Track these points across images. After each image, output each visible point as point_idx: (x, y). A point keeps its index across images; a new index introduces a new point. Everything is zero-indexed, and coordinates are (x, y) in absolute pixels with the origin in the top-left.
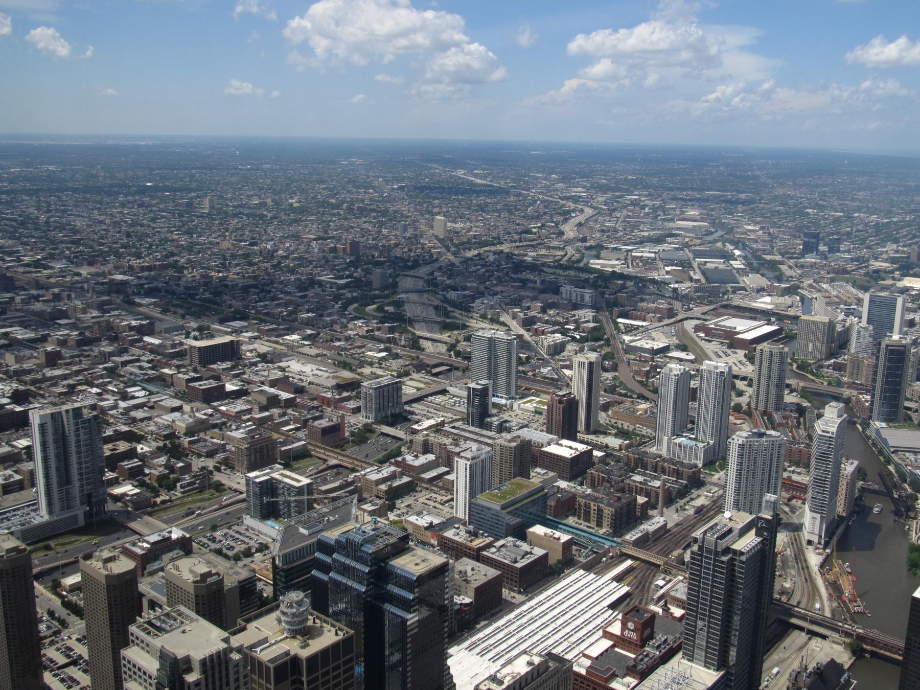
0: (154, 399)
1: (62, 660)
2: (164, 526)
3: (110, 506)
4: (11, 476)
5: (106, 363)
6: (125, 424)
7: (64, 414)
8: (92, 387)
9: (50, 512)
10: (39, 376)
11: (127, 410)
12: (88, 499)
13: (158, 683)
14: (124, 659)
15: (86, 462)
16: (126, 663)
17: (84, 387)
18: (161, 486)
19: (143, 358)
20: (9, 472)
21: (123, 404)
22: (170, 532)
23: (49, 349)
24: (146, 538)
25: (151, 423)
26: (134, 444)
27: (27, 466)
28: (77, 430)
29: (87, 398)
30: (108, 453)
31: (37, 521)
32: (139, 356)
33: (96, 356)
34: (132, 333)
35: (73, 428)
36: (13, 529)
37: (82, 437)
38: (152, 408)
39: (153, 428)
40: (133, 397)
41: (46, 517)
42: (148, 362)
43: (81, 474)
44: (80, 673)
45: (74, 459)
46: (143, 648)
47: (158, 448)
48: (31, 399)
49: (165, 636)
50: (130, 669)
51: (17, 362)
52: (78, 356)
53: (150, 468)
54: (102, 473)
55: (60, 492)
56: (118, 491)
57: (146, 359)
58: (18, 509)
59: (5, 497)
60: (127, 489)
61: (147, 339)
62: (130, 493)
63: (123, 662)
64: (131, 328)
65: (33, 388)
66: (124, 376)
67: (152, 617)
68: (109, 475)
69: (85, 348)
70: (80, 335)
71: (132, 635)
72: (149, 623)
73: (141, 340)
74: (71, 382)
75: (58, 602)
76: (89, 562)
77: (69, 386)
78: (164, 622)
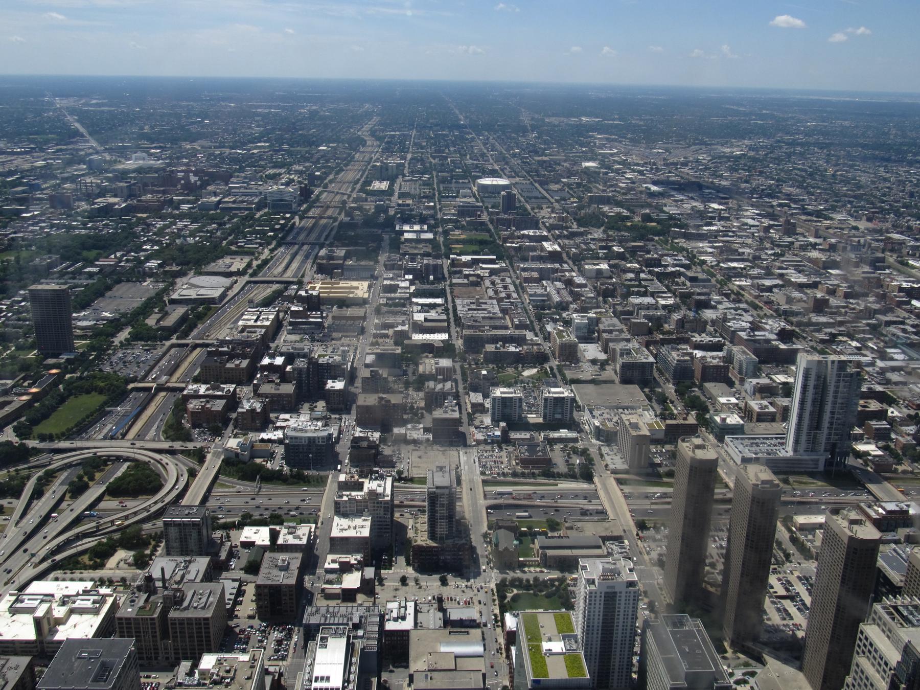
0: (913, 365)
1: (782, 592)
2: (901, 497)
3: (851, 461)
4: (766, 407)
5: (870, 319)
6: (879, 384)
7: (829, 364)
8: (852, 340)
9: (795, 450)
10: (805, 320)
11: (883, 371)
12: (832, 448)
13: (894, 675)
14: (862, 633)
15: (839, 413)
16: (863, 638)
17: (845, 339)
18: (904, 455)
19: (908, 321)
20: (765, 402)
21: (880, 364)
22: (908, 506)
23: (819, 295)
24: (883, 504)
25: (906, 388)
26: (885, 406)
27: (784, 402)
28: (838, 381)
29: (847, 351)
30: (860, 409)
31: (782, 454)
32: (904, 318)
33: (861, 311)
34: (901, 294)
35: (834, 379)
36: (760, 455)
37: (841, 389)
38: (909, 373)
39: (906, 394)
40: (892, 359)
41: (790, 454)
42: (913, 326)
43: (831, 423)
44: (795, 609)
45: (828, 408)
46: (883, 631)
47: (909, 416)
48: (794, 339)
49: (911, 629)
50: (865, 646)
51: (787, 303)
52: (844, 307)
53: (897, 433)
54: (852, 428)
55: (809, 434)
56: (861, 447)
57: (911, 323)
58: (767, 439)
59: (758, 424)
60: (871, 448)
61: (914, 302)
62: (873, 453)
63: (859, 635)
64: (901, 289)
65: (797, 330)
66: (886, 336)
67: (899, 603)
68: (857, 431)
69: (851, 301)
70: (849, 287)
71: (875, 613)
72: (895, 608)
73: (909, 303)
74: (833, 331)
75: (787, 535)
76: (835, 517)
77: (831, 334)
78: (912, 614)
